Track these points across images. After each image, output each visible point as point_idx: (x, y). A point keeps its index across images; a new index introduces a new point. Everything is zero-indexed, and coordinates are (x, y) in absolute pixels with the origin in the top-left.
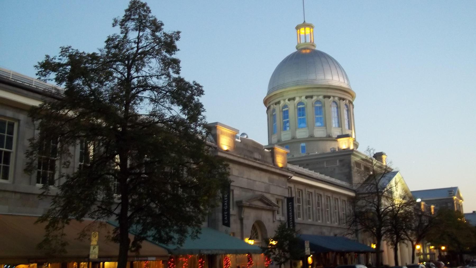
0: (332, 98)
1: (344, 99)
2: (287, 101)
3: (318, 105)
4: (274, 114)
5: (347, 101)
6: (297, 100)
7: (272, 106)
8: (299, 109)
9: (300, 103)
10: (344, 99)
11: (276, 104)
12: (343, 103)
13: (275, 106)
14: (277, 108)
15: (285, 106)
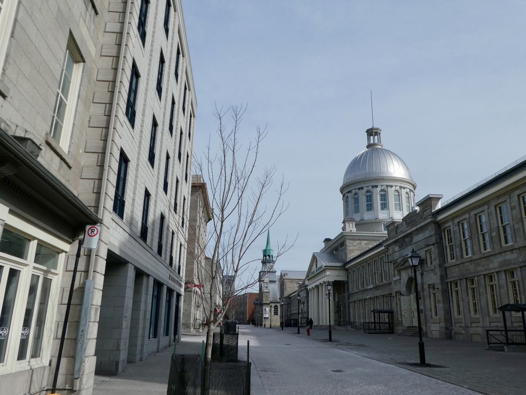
0: (394, 187)
1: (404, 188)
2: (357, 190)
3: (382, 193)
4: (347, 200)
5: (408, 190)
6: (365, 189)
8: (367, 196)
9: (368, 191)
10: (404, 188)
11: (348, 192)
13: (348, 194)
14: (350, 195)
15: (356, 194)
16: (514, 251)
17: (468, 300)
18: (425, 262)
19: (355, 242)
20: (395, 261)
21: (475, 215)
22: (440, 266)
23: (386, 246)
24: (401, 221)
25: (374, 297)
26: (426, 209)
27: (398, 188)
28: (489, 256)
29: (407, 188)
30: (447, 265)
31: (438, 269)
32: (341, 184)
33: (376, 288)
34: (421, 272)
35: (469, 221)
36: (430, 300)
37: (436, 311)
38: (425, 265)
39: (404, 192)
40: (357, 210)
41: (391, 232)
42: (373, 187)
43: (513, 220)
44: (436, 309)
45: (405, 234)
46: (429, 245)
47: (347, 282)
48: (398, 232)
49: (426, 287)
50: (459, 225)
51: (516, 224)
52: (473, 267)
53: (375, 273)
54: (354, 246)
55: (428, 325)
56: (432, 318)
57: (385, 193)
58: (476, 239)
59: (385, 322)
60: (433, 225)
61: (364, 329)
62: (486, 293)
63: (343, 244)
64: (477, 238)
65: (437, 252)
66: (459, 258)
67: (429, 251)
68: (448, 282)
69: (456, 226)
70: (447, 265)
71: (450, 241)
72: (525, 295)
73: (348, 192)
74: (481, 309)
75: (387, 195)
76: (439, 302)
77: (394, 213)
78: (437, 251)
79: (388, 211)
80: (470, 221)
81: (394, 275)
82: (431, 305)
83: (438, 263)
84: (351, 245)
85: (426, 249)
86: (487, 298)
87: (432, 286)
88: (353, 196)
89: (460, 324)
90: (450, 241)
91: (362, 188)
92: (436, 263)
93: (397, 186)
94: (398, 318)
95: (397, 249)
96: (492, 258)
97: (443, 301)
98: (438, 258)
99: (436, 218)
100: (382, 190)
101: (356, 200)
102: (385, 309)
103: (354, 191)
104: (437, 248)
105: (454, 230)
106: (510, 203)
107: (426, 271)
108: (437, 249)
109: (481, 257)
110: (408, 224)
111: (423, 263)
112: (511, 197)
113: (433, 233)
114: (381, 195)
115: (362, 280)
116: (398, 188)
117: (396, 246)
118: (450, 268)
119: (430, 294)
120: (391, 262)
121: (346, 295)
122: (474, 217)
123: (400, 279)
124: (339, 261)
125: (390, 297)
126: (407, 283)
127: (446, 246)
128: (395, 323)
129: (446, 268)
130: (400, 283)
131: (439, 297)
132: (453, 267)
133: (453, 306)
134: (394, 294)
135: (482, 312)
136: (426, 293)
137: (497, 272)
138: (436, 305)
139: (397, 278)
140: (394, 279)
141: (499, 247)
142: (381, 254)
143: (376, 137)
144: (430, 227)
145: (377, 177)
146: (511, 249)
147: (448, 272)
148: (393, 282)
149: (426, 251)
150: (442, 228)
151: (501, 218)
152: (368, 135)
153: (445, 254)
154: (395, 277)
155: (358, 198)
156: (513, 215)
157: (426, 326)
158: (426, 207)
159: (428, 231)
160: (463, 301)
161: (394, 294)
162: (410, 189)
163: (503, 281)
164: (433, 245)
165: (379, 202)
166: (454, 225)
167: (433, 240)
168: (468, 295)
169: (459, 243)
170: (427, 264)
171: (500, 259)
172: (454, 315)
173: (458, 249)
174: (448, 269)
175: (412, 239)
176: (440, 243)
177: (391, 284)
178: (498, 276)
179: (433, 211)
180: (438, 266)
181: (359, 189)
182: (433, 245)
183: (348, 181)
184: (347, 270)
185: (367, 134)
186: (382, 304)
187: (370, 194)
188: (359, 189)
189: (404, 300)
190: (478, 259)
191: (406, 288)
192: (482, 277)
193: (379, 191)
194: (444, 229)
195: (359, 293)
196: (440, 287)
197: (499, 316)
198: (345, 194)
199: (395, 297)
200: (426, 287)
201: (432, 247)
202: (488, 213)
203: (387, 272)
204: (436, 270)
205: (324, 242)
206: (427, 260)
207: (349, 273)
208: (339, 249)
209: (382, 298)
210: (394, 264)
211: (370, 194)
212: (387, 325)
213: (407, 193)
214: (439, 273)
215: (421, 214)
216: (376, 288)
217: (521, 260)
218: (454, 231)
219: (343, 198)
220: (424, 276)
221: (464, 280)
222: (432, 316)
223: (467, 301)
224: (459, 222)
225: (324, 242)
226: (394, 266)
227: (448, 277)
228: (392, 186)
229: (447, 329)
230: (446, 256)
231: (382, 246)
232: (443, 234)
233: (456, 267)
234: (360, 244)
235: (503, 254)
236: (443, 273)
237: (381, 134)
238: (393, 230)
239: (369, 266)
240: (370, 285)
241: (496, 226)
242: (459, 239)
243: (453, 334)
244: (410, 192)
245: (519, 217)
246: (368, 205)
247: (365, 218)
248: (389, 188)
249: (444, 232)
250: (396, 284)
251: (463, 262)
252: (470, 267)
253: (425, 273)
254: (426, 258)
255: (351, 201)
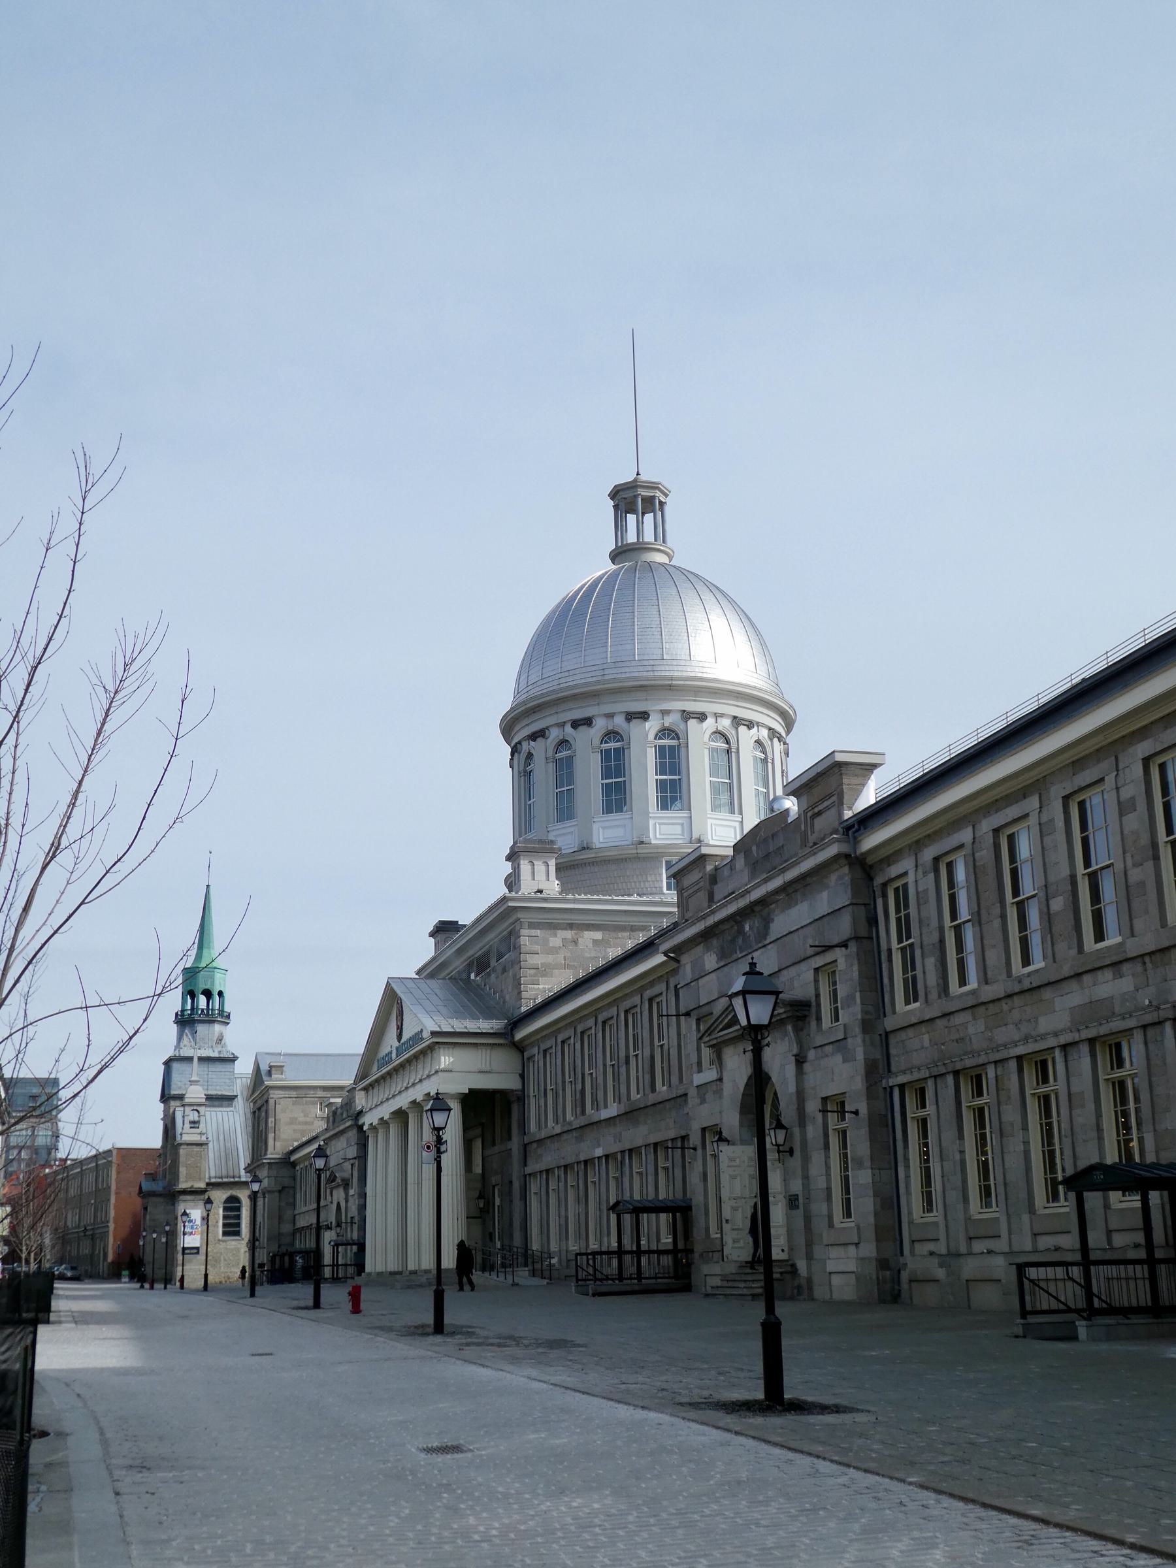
0: (710, 721)
1: (750, 725)
2: (568, 728)
5: (764, 733)
6: (600, 725)
7: (525, 745)
8: (606, 755)
9: (612, 734)
10: (750, 725)
11: (534, 737)
12: (746, 738)
13: (532, 743)
14: (539, 748)
15: (563, 743)
16: (1126, 968)
17: (962, 1152)
18: (814, 1010)
19: (556, 935)
20: (704, 1010)
21: (996, 831)
22: (867, 1026)
23: (672, 950)
24: (730, 852)
25: (623, 1152)
26: (821, 807)
27: (725, 723)
28: (1039, 987)
29: (758, 724)
30: (890, 1023)
31: (859, 1040)
32: (504, 703)
33: (631, 1115)
34: (795, 1051)
35: (973, 854)
36: (827, 1157)
37: (848, 1200)
38: (813, 1023)
39: (746, 738)
40: (566, 808)
41: (690, 896)
42: (630, 716)
43: (1124, 852)
44: (848, 1192)
45: (742, 903)
46: (828, 948)
47: (520, 1097)
48: (716, 898)
49: (812, 1106)
50: (936, 871)
51: (1135, 865)
52: (982, 1028)
53: (627, 1058)
54: (553, 951)
55: (818, 1251)
56: (831, 1225)
57: (674, 742)
58: (997, 923)
59: (661, 1248)
60: (846, 869)
61: (577, 1281)
62: (1025, 1128)
63: (510, 941)
64: (999, 919)
65: (856, 975)
66: (934, 995)
67: (828, 971)
68: (891, 1088)
69: (925, 874)
70: (890, 1023)
71: (904, 930)
72: (1155, 1130)
73: (534, 737)
74: (1005, 1184)
75: (683, 750)
76: (859, 1164)
77: (709, 822)
78: (856, 968)
79: (685, 814)
80: (977, 855)
81: (699, 1063)
82: (828, 1175)
83: (859, 1017)
84: (537, 948)
85: (819, 961)
86: (1026, 1143)
87: (836, 1105)
88: (550, 753)
89: (931, 1246)
90: (904, 930)
91: (588, 722)
92: (851, 1015)
93: (722, 715)
94: (707, 1229)
95: (710, 961)
96: (1047, 994)
97: (872, 1159)
98: (858, 995)
99: (856, 842)
100: (665, 732)
101: (564, 769)
102: (661, 1198)
103: (554, 734)
104: (859, 960)
105: (920, 889)
106: (1117, 788)
107: (815, 1048)
108: (856, 962)
109: (1009, 992)
110: (754, 866)
111: (805, 1016)
112: (1121, 766)
113: (844, 899)
114: (661, 751)
115: (579, 1087)
116: (725, 723)
117: (708, 949)
118: (903, 1035)
119: (826, 1135)
120: (688, 1014)
121: (515, 1145)
122: (991, 841)
123: (720, 1080)
124: (488, 1014)
125: (683, 1148)
126: (743, 1094)
127: (890, 951)
128: (698, 1248)
129: (887, 1034)
130: (719, 1093)
131: (860, 1144)
132: (910, 1033)
133: (908, 1177)
134: (695, 1139)
135: (1006, 1199)
136: (813, 1131)
137: (1065, 1047)
138: (847, 1178)
139: (710, 1075)
140: (699, 1079)
141: (1074, 952)
142: (652, 984)
143: (649, 518)
144: (833, 878)
145: (647, 679)
146: (1115, 959)
147: (893, 1051)
148: (692, 1093)
149: (817, 970)
150: (879, 880)
151: (1085, 842)
152: (616, 507)
153: (886, 981)
154: (700, 1071)
155: (570, 759)
156: (1126, 832)
157: (809, 1257)
158: (823, 800)
159: (825, 894)
160: (942, 1159)
161: (695, 1139)
162: (770, 729)
163: (1083, 1083)
164: (844, 945)
165: (652, 777)
166: (920, 870)
167: (844, 927)
168: (961, 1136)
169: (935, 937)
170: (819, 1019)
171: (1073, 998)
172: (910, 1213)
173: (931, 962)
174: (893, 1040)
175: (767, 922)
176: (871, 938)
177: (686, 1101)
178: (1066, 1061)
179: (848, 814)
180: (857, 1030)
181: (576, 724)
182: (844, 945)
183: (535, 691)
184: (519, 1048)
185: (612, 504)
186: (651, 1179)
187: (618, 745)
188: (576, 724)
189: (732, 1159)
190: (999, 1000)
191: (741, 1113)
192: (1013, 1065)
193: (651, 737)
194: (885, 885)
195: (565, 1136)
196: (863, 1110)
197: (1067, 1210)
198: (519, 743)
199: (700, 1151)
200: (812, 1106)
201: (839, 954)
202: (1040, 824)
203: (674, 1052)
204: (850, 1040)
205: (432, 935)
206: (818, 1005)
207: (528, 1059)
208: (493, 963)
209: (651, 1156)
210: (698, 1021)
211: (618, 745)
212: (667, 1260)
213: (759, 742)
214: (860, 1055)
215: (803, 827)
216: (631, 1115)
217: (1147, 1002)
218: (918, 893)
219: (512, 759)
220: (807, 1067)
221: (950, 1079)
222: (830, 1217)
223: (958, 1157)
224: (936, 860)
225: (432, 935)
226: (698, 1030)
227: (893, 1069)
228: (702, 717)
229: (883, 1264)
230: (887, 989)
231: (656, 952)
232: (880, 902)
233: (923, 1028)
234: (575, 942)
235: (1087, 978)
236: (878, 1055)
237: (667, 508)
238: (699, 890)
239: (604, 1030)
240: (606, 1107)
241: (1065, 872)
242: (934, 923)
243: (905, 1285)
244: (771, 740)
245: (1145, 839)
246: (607, 789)
247: (595, 840)
248: (692, 723)
249: (885, 896)
250: (703, 1101)
251: (947, 1010)
252: (971, 1030)
253: (811, 1055)
254: (818, 996)
255: (543, 772)
